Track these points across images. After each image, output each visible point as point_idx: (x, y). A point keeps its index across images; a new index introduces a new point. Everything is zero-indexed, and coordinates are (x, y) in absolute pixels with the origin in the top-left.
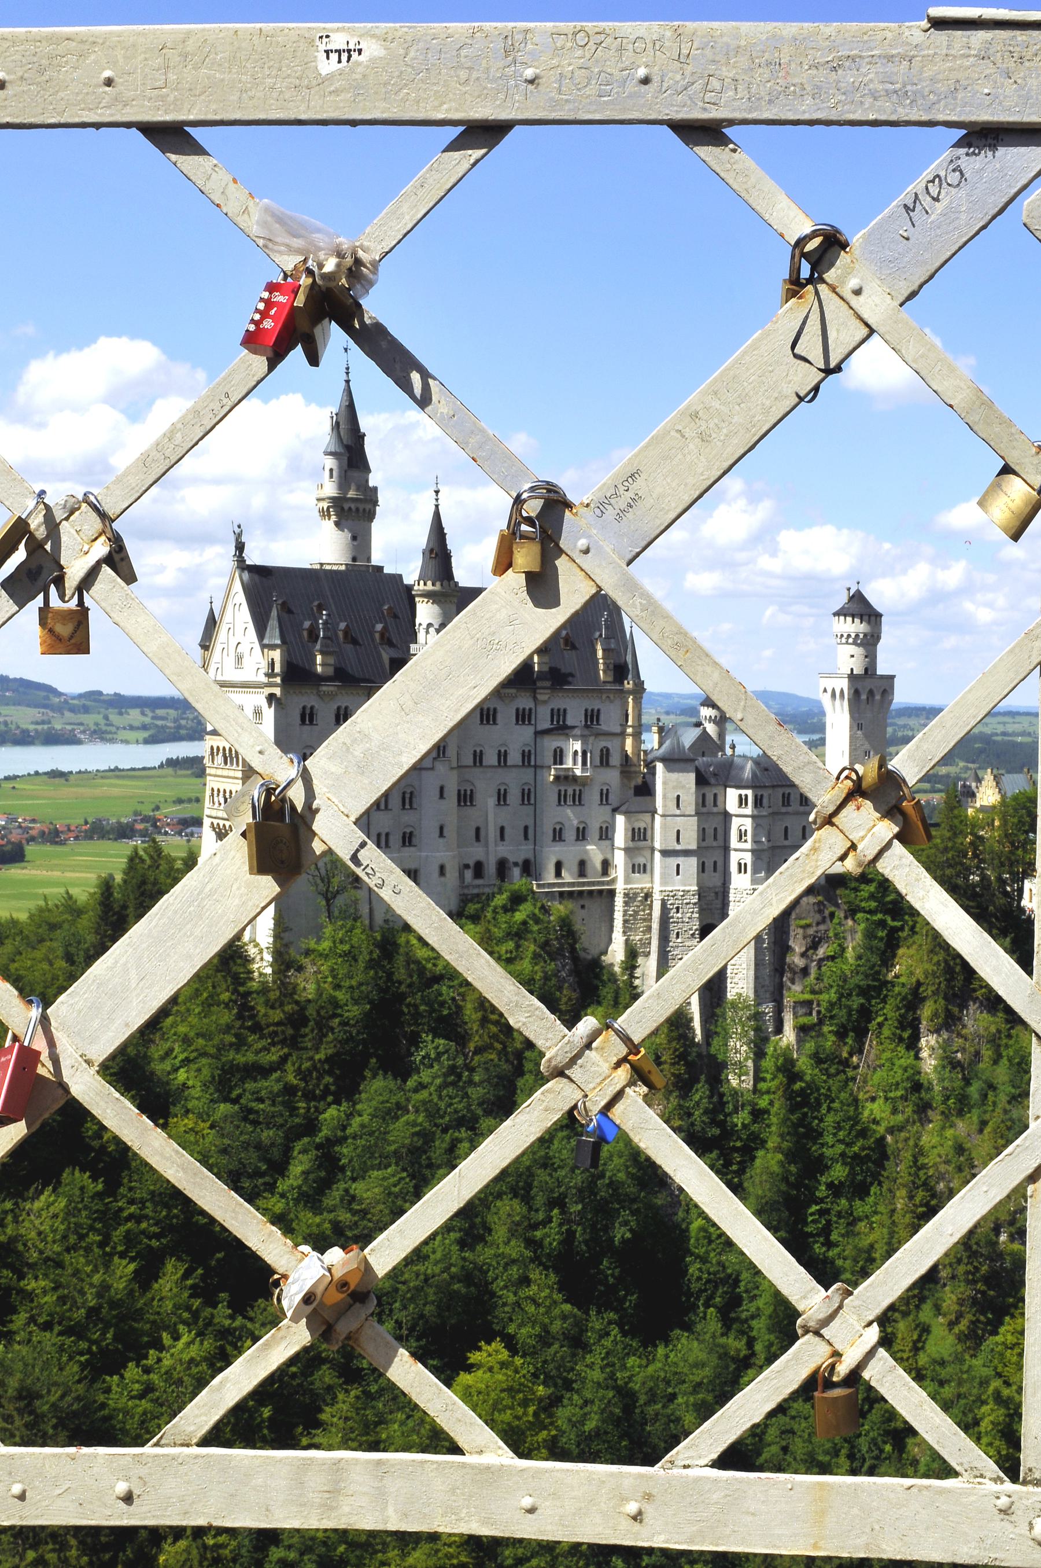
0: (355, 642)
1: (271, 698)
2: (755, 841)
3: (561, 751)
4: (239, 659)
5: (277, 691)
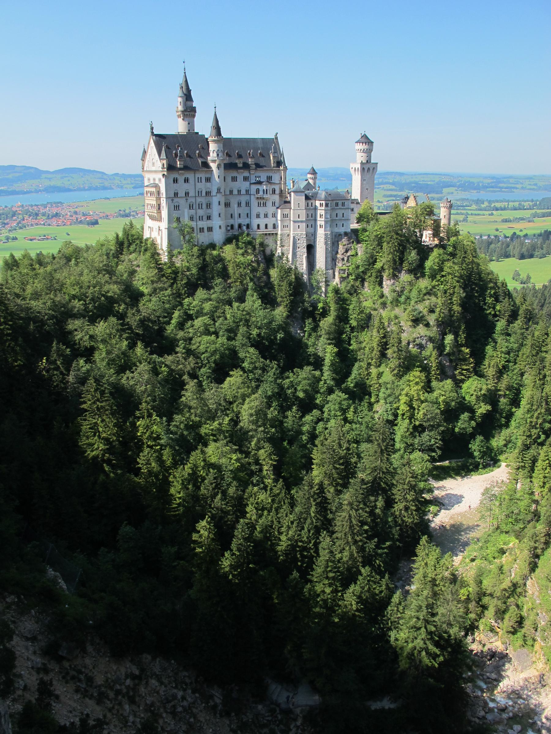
1: (164, 175)
2: (325, 218)
4: (153, 164)
5: (166, 173)
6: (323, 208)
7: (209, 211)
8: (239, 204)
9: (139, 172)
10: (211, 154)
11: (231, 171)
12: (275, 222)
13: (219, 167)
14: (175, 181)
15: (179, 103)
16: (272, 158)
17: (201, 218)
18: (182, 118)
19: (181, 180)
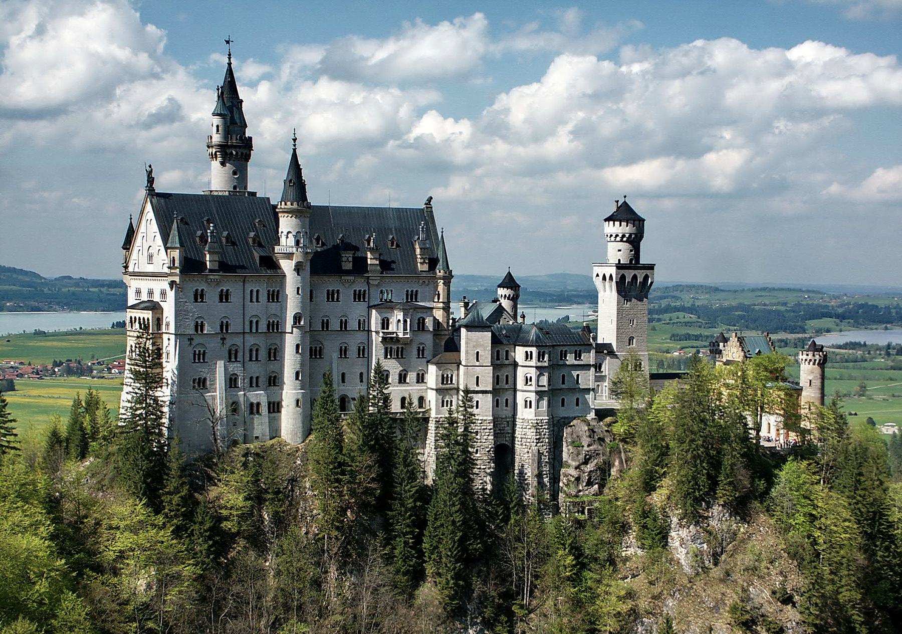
0: (234, 244)
1: (172, 284)
3: (388, 320)
4: (150, 257)
5: (177, 279)
6: (533, 363)
7: (273, 366)
8: (343, 352)
9: (115, 274)
10: (283, 240)
11: (326, 278)
12: (423, 394)
13: (298, 268)
14: (199, 296)
15: (215, 129)
16: (418, 251)
17: (254, 383)
18: (219, 159)
19: (212, 295)
